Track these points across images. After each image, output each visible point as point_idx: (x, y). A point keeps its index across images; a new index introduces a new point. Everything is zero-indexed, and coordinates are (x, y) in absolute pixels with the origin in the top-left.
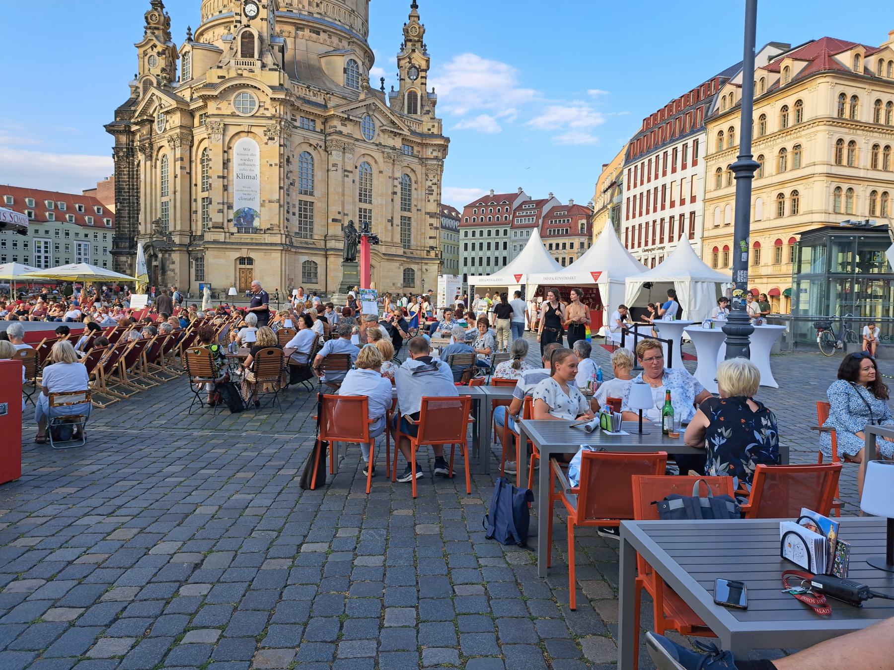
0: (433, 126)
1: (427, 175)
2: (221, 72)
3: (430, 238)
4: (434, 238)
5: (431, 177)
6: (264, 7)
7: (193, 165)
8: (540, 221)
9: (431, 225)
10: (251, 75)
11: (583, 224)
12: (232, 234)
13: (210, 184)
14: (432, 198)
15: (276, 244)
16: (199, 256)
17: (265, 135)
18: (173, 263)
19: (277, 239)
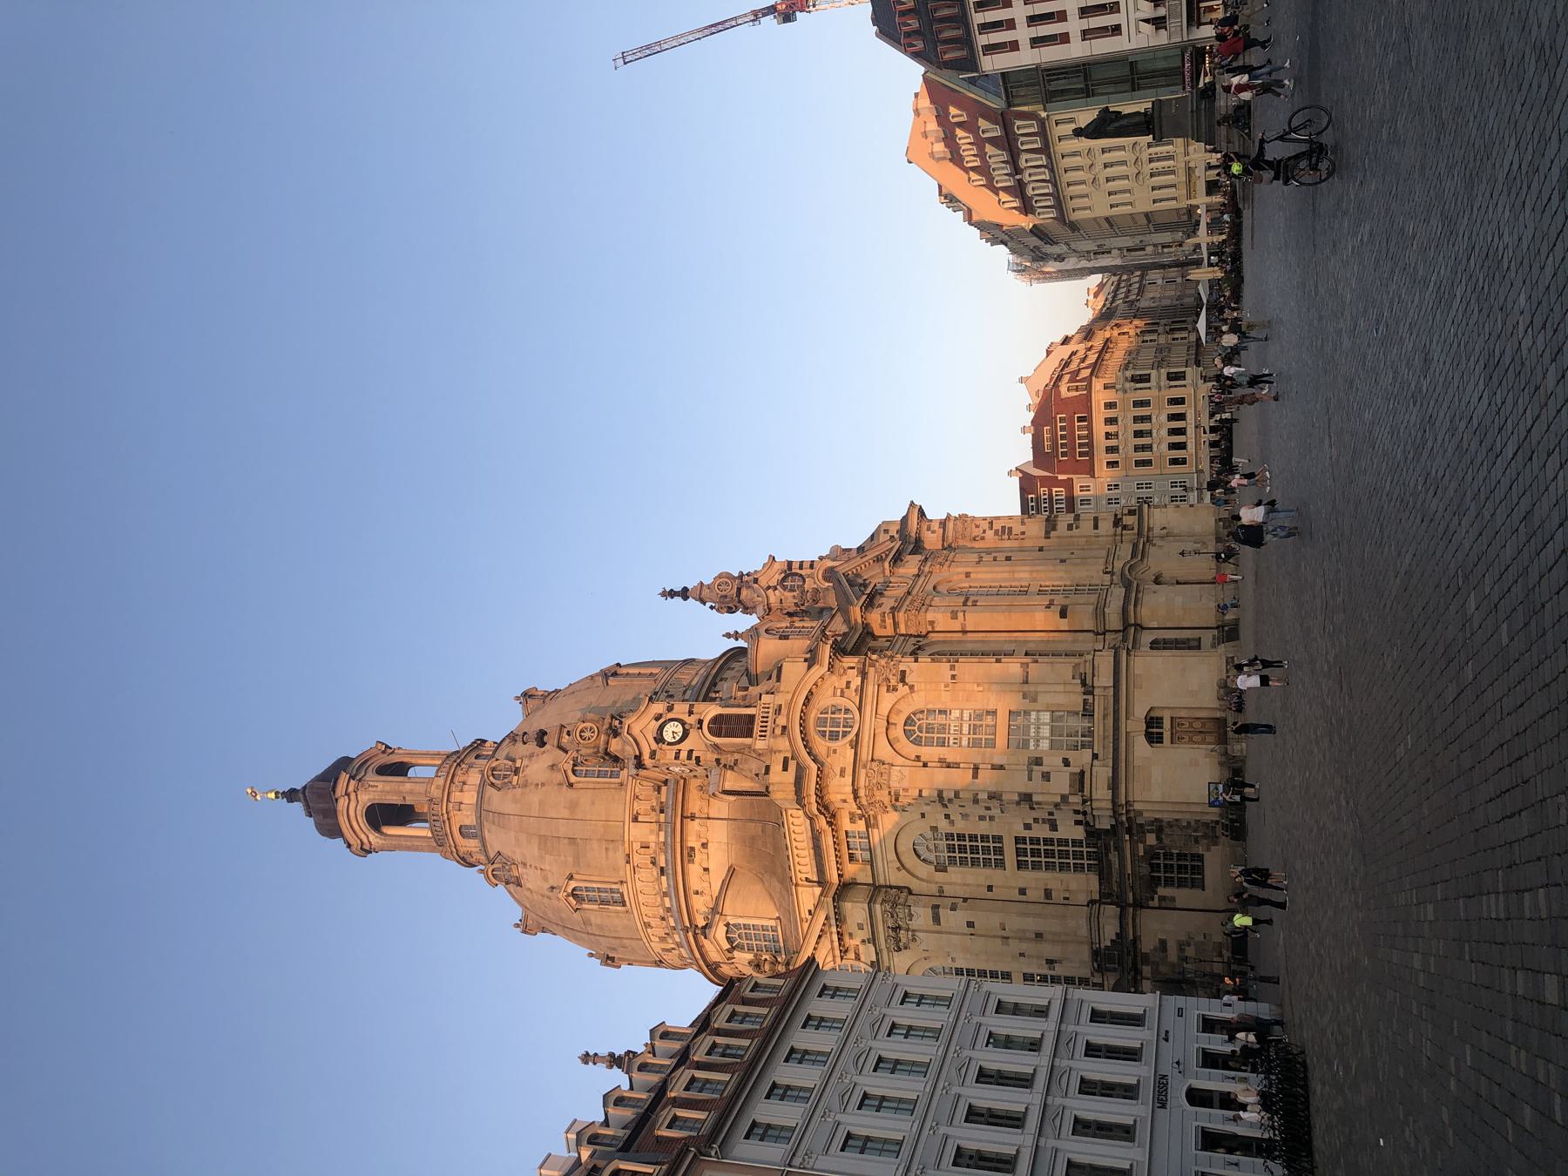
0: (886, 531)
2: (777, 767)
3: (1096, 527)
4: (1096, 520)
5: (976, 532)
6: (670, 709)
7: (948, 891)
8: (1061, 477)
9: (1070, 527)
10: (784, 711)
12: (1095, 756)
13: (992, 796)
16: (1145, 869)
17: (895, 689)
18: (1163, 943)
19: (1105, 662)
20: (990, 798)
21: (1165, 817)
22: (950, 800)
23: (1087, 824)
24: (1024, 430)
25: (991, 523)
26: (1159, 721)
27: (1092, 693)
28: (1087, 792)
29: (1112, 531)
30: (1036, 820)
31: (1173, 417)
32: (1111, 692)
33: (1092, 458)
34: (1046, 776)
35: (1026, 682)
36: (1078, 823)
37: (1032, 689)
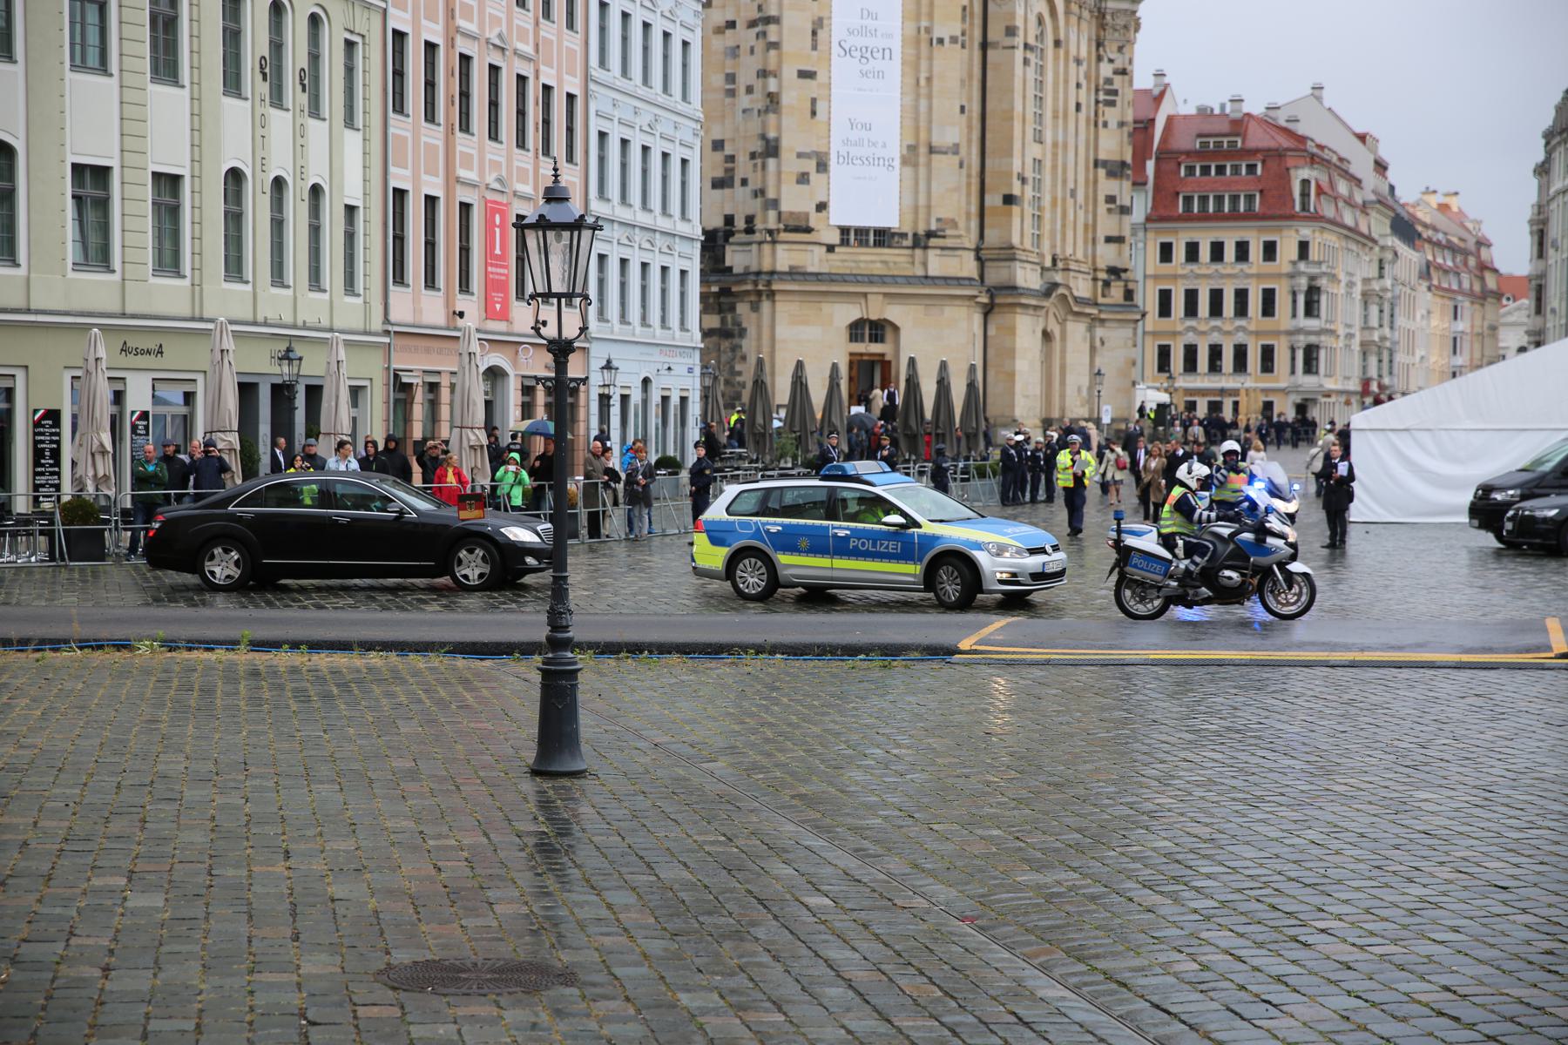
1: (1099, 44)
3: (1109, 240)
4: (1119, 240)
8: (1150, 166)
9: (1111, 199)
11: (1305, 183)
12: (831, 249)
13: (773, 100)
14: (1111, 115)
15: (958, 281)
20: (770, 95)
21: (748, 345)
22: (764, 34)
23: (729, 234)
24: (1237, 101)
25: (1123, 72)
26: (877, 338)
27: (916, 245)
28: (784, 236)
29: (1101, 264)
30: (731, 159)
31: (1241, 353)
32: (920, 272)
33: (1179, 219)
34: (803, 178)
35: (932, 150)
36: (729, 220)
37: (922, 160)
